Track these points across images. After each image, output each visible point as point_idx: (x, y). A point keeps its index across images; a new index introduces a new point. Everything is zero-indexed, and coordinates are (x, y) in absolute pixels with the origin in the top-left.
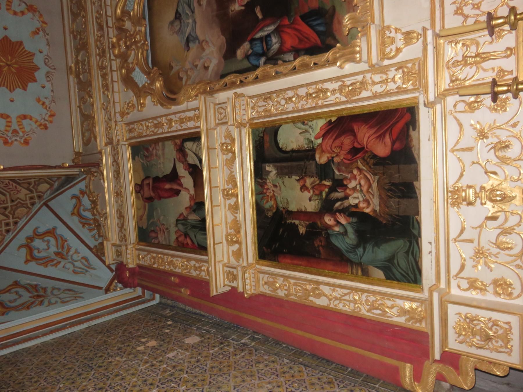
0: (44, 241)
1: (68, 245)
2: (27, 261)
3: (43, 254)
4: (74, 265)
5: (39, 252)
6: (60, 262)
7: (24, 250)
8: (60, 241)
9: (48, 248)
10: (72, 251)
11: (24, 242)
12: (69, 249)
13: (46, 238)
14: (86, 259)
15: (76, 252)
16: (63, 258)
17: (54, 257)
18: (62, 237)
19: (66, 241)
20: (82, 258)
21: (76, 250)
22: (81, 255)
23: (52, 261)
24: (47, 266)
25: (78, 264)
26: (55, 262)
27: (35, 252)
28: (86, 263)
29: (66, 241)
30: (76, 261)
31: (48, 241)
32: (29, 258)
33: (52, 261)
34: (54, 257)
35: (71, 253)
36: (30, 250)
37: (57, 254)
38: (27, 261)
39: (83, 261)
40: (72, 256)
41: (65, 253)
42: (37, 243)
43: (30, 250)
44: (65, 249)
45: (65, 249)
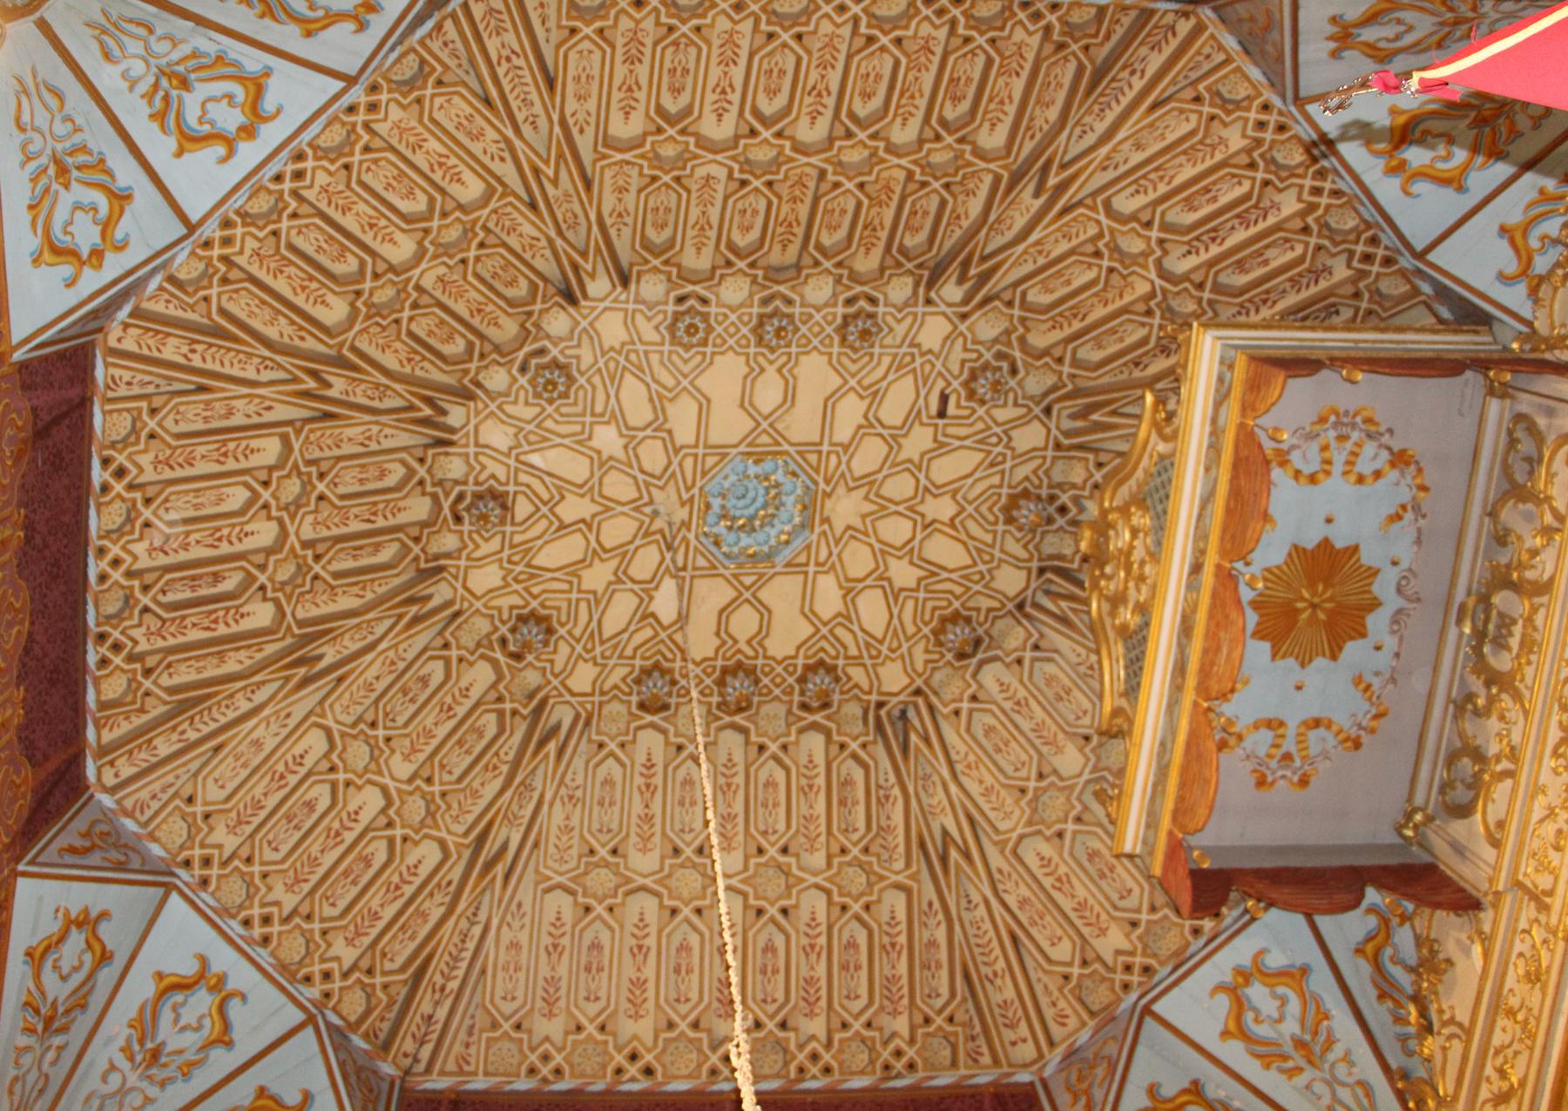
0: (1274, 996)
1: (1330, 1031)
2: (1225, 1034)
3: (1263, 1031)
4: (1334, 1093)
5: (1256, 1020)
6: (1300, 1070)
7: (1223, 1002)
8: (1312, 1009)
9: (1280, 1020)
10: (1337, 1051)
11: (1228, 978)
12: (1330, 1042)
13: (1281, 990)
14: (1369, 1094)
15: (1347, 1058)
16: (1311, 1062)
17: (1288, 1048)
18: (1318, 1002)
19: (1327, 1017)
20: (1360, 1083)
21: (1348, 1053)
22: (1358, 1073)
23: (1285, 1058)
24: (1267, 1067)
25: (1344, 1094)
26: (1290, 1064)
27: (1249, 1017)
28: (1365, 1101)
29: (1327, 1017)
30: (1343, 1084)
31: (1284, 1001)
32: (1232, 1026)
33: (1285, 1058)
34: (1288, 1048)
35: (1331, 1057)
36: (1239, 1005)
37: (1300, 1044)
38: (1225, 1034)
39: (1359, 1091)
40: (1333, 1066)
41: (1317, 1049)
42: (1257, 993)
43: (1239, 1005)
44: (1322, 1038)
45: (1322, 1038)
